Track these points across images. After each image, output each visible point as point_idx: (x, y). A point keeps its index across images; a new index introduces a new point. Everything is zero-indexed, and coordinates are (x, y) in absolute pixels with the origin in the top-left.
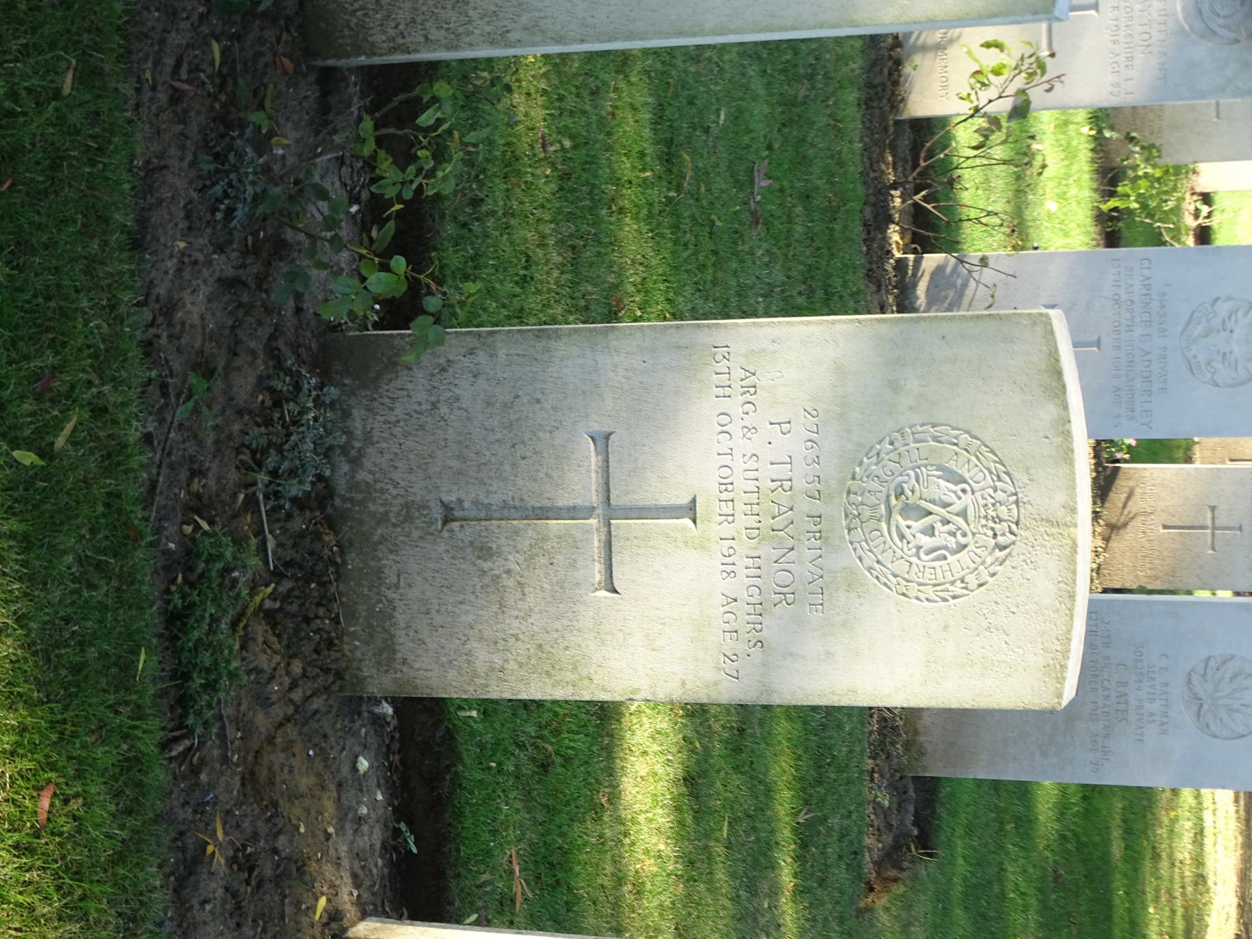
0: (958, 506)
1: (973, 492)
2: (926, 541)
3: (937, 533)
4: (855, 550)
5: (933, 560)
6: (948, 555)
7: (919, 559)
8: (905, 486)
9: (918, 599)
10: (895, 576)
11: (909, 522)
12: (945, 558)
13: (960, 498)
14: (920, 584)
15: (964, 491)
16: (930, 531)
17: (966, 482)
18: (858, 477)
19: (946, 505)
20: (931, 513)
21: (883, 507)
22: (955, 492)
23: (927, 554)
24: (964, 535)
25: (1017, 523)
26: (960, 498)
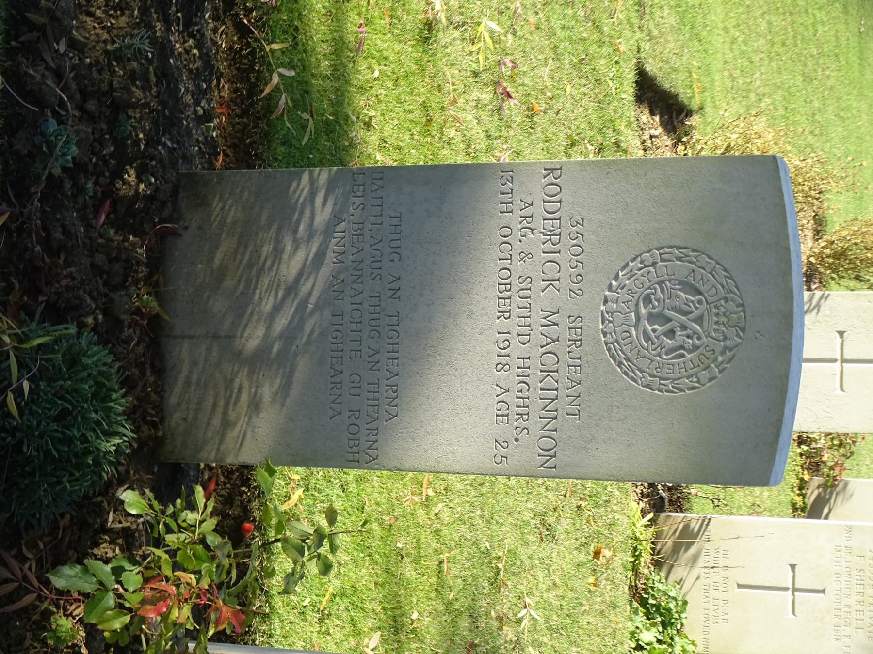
3: (677, 338)
7: (660, 357)
8: (653, 297)
9: (660, 390)
10: (642, 371)
11: (656, 327)
13: (697, 308)
14: (661, 379)
15: (700, 302)
16: (671, 333)
17: (700, 293)
18: (614, 289)
19: (685, 313)
20: (669, 320)
21: (633, 314)
22: (692, 302)
23: (666, 355)
24: (699, 338)
26: (697, 308)
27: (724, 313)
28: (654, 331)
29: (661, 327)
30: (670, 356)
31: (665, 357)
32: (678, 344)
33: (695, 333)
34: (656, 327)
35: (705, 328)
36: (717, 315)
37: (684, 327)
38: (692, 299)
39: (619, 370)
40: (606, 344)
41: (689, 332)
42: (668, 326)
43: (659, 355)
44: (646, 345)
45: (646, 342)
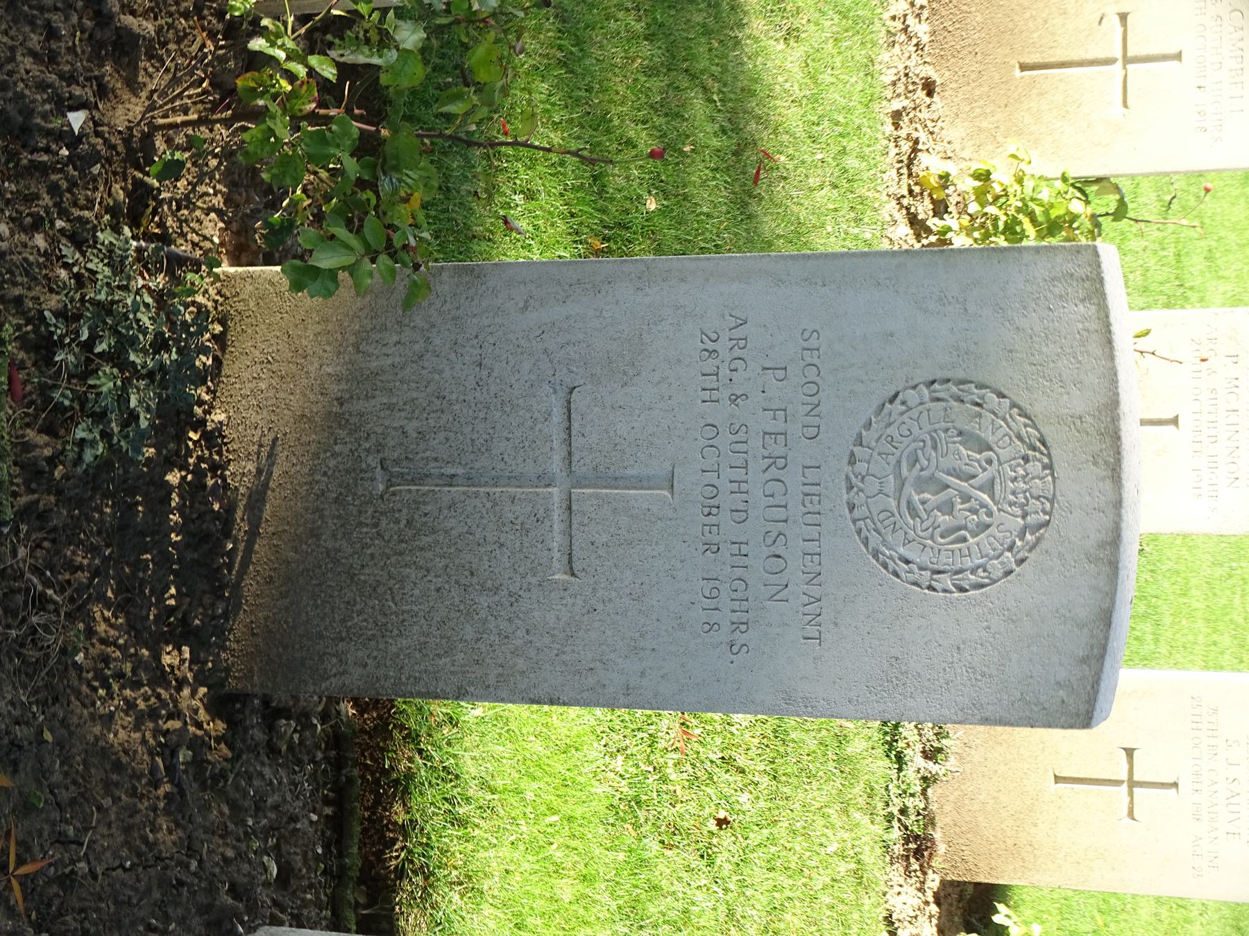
0: (983, 477)
1: (1000, 464)
2: (944, 519)
3: (956, 513)
4: (859, 532)
5: (952, 543)
6: (968, 536)
11: (926, 496)
12: (964, 540)
13: (985, 470)
16: (948, 508)
20: (947, 487)
22: (978, 461)
23: (942, 537)
24: (990, 514)
25: (1052, 502)
27: (1024, 477)
28: (923, 503)
29: (933, 495)
30: (947, 540)
31: (942, 541)
32: (956, 523)
33: (983, 505)
34: (926, 496)
35: (997, 498)
36: (1014, 480)
37: (966, 498)
38: (978, 456)
39: (874, 561)
40: (854, 521)
41: (973, 503)
42: (943, 496)
43: (932, 538)
44: (912, 522)
45: (913, 518)
